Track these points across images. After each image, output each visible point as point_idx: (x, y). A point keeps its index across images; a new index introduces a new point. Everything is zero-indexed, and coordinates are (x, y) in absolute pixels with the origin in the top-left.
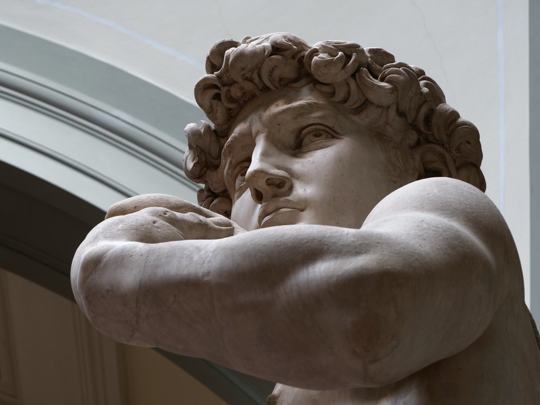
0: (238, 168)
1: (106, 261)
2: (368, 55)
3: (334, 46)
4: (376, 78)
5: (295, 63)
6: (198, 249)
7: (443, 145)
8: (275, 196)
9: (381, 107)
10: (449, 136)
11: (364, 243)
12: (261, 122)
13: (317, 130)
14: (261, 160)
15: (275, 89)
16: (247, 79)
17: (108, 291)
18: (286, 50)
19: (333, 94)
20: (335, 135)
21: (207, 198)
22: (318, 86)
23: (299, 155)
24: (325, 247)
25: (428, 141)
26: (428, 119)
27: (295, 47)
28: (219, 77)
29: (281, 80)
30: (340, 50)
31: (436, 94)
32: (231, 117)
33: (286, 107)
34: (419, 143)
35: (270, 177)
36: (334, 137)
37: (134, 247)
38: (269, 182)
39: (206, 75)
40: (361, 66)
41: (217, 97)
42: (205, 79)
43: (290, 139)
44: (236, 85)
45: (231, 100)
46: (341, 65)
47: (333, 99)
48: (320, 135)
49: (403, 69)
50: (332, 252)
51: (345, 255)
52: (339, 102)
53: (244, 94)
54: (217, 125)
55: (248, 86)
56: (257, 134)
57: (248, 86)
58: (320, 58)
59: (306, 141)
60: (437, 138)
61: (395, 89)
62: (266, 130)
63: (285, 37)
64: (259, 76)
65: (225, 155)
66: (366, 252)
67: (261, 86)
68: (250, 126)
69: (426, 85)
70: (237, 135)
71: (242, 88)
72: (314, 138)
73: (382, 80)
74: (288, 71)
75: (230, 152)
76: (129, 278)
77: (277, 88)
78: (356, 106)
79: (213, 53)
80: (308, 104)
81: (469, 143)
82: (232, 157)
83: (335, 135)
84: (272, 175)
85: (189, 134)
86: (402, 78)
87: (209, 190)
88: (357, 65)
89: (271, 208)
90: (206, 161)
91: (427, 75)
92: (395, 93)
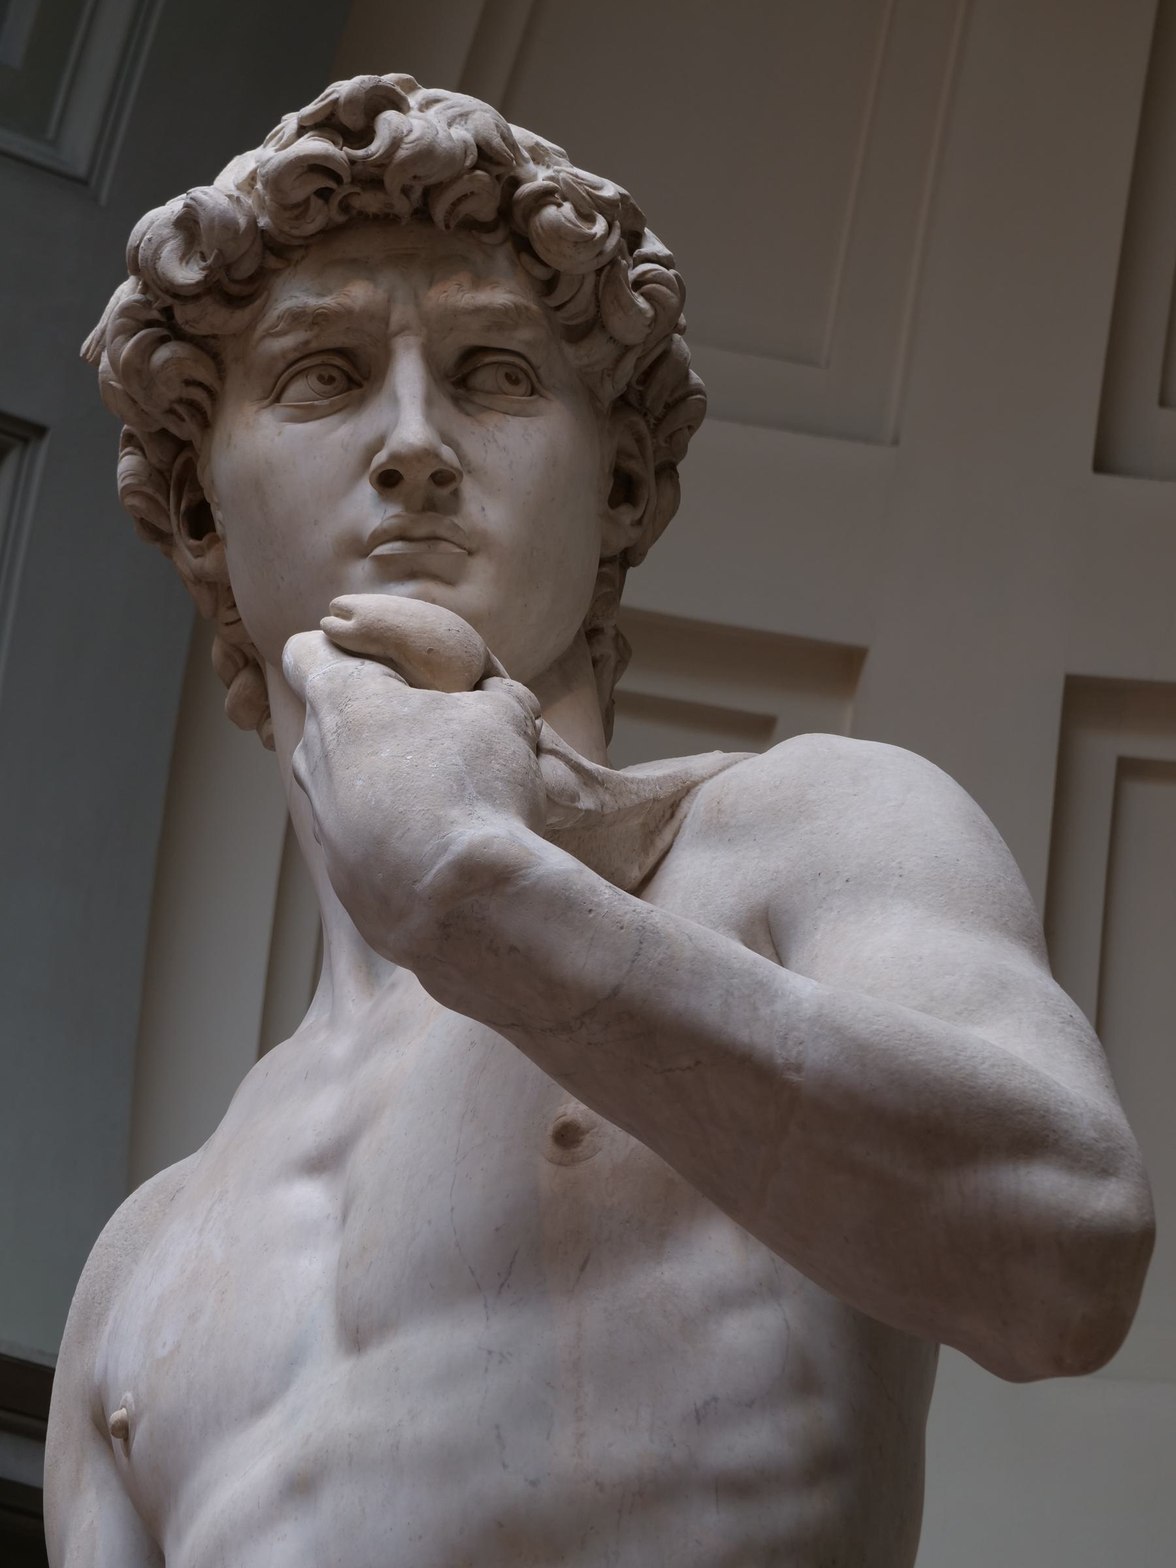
0: (317, 360)
3: (588, 193)
7: (645, 415)
8: (430, 506)
10: (670, 407)
15: (443, 228)
17: (513, 949)
18: (499, 164)
20: (537, 385)
21: (149, 324)
22: (525, 258)
28: (353, 162)
35: (443, 467)
36: (533, 392)
37: (593, 890)
41: (324, 194)
42: (327, 157)
48: (515, 382)
49: (676, 276)
56: (403, 329)
57: (402, 206)
58: (570, 221)
59: (485, 379)
60: (648, 404)
61: (655, 319)
68: (389, 301)
72: (507, 386)
74: (485, 209)
75: (314, 324)
76: (585, 962)
77: (447, 226)
78: (574, 322)
84: (445, 463)
85: (212, 220)
87: (168, 311)
89: (422, 530)
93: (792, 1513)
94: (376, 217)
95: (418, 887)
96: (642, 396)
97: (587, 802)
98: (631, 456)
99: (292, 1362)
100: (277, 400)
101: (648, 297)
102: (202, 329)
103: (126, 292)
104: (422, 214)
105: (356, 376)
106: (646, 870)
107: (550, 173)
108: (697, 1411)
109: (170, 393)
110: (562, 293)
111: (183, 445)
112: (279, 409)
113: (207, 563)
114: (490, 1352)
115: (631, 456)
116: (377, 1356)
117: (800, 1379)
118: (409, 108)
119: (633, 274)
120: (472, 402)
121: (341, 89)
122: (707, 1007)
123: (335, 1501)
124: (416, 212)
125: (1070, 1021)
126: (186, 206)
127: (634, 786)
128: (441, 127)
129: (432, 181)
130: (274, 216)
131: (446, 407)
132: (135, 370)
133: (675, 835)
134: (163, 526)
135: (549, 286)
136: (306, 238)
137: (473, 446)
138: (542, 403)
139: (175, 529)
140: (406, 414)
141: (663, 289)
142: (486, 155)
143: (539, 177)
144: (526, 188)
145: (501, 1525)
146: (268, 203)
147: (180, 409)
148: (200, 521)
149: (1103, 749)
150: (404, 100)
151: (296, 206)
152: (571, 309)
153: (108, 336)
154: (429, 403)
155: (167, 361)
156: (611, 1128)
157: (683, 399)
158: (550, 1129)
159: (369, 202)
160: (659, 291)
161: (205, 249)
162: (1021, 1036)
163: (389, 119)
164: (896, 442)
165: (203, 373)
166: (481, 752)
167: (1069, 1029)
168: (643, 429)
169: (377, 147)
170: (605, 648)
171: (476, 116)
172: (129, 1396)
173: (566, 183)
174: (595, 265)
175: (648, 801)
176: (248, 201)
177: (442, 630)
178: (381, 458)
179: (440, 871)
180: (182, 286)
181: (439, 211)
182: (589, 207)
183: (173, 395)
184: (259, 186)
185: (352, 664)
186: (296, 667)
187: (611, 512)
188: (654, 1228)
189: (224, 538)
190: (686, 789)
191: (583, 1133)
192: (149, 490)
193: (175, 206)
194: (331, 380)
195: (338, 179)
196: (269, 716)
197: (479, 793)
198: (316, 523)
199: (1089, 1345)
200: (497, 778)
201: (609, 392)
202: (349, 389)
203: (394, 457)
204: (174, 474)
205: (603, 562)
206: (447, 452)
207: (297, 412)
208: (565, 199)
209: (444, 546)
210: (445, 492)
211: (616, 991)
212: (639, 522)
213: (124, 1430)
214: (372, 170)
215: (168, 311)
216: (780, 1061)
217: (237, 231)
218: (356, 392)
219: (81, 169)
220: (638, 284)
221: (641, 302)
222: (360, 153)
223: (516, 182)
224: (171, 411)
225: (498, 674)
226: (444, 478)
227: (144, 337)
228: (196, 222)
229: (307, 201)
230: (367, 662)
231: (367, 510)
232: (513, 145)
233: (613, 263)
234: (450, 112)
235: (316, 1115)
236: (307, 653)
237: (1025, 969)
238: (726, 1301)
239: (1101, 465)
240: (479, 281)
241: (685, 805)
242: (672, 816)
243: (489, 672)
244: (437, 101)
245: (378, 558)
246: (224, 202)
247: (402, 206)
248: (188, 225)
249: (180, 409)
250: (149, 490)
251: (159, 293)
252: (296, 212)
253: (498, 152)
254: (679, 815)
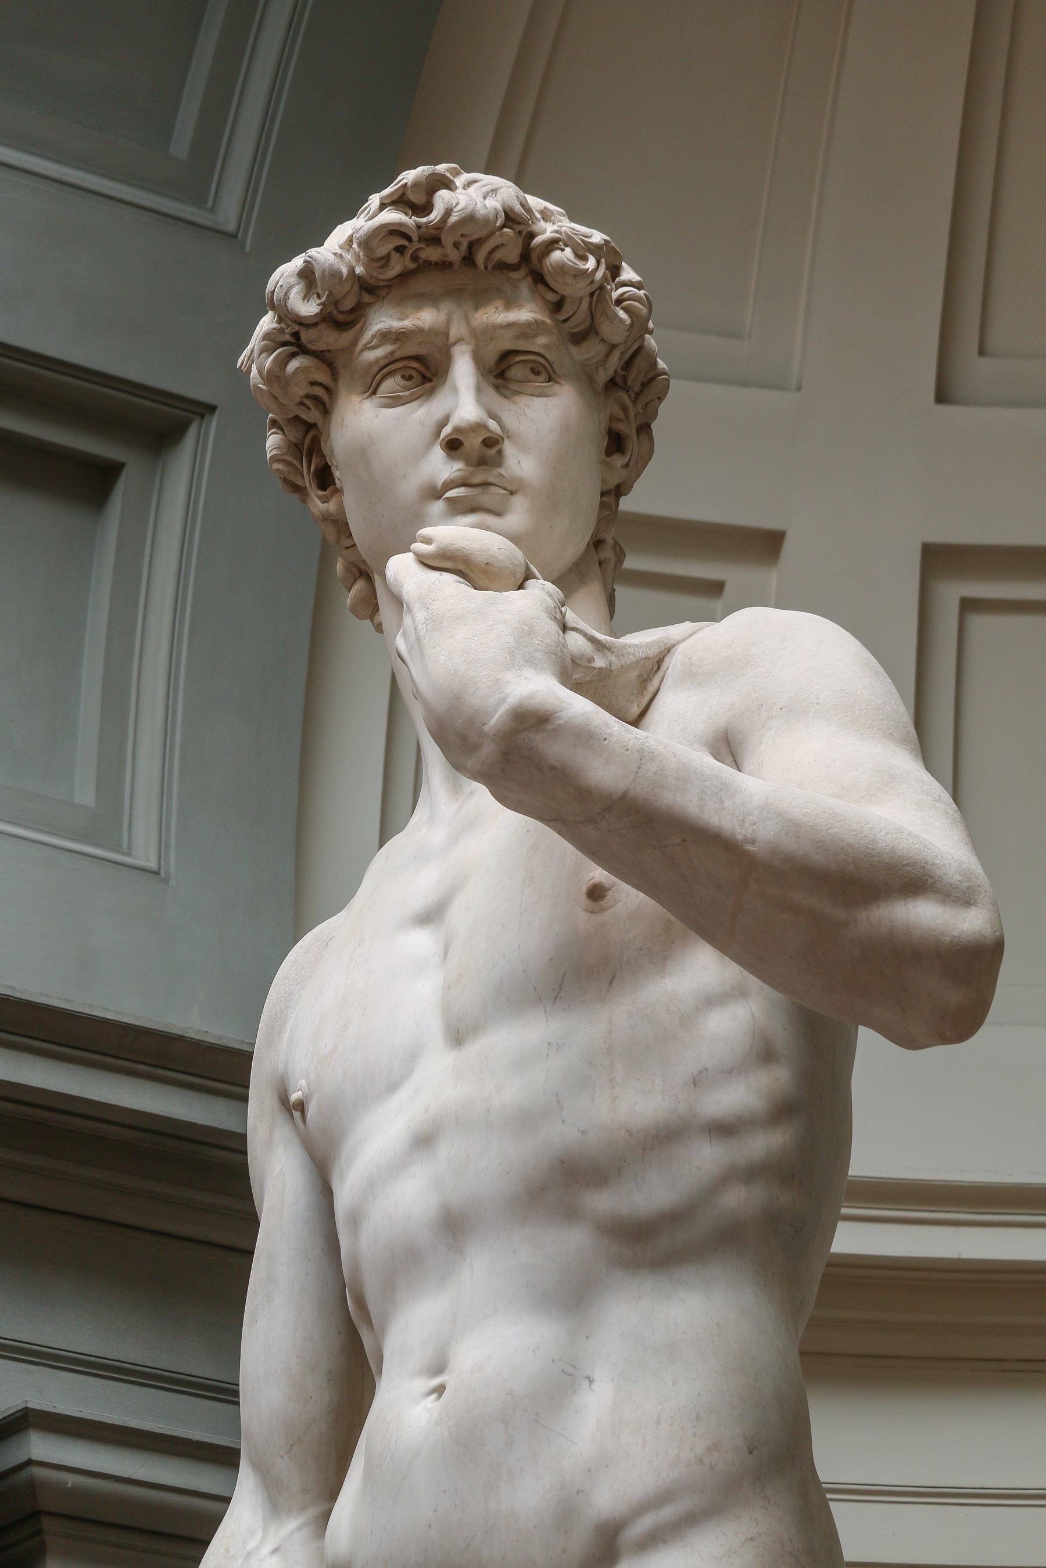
1: (560, 725)
3: (582, 240)
8: (482, 462)
10: (646, 385)
12: (468, 323)
17: (553, 768)
18: (519, 223)
20: (553, 375)
21: (284, 344)
22: (541, 287)
23: (507, 392)
24: (930, 881)
28: (419, 226)
36: (550, 379)
37: (607, 725)
41: (400, 250)
42: (401, 224)
44: (439, 250)
48: (537, 373)
50: (937, 891)
56: (459, 341)
57: (454, 256)
59: (516, 372)
60: (629, 383)
61: (632, 325)
70: (426, 328)
72: (532, 376)
74: (512, 255)
76: (604, 774)
77: (486, 268)
78: (576, 330)
79: (416, 184)
82: (399, 348)
85: (324, 270)
87: (296, 335)
89: (478, 479)
93: (763, 1144)
94: (436, 263)
95: (486, 728)
96: (625, 378)
97: (600, 663)
98: (619, 420)
99: (412, 1057)
100: (374, 393)
101: (626, 310)
102: (320, 346)
103: (267, 322)
104: (469, 260)
105: (428, 374)
106: (642, 707)
107: (555, 227)
108: (694, 1078)
109: (300, 390)
110: (567, 311)
111: (310, 426)
112: (376, 399)
113: (331, 506)
114: (549, 1044)
115: (619, 420)
116: (473, 1049)
117: (765, 1054)
118: (456, 188)
119: (615, 295)
120: (509, 389)
121: (409, 176)
122: (690, 803)
123: (448, 1150)
124: (464, 259)
125: (939, 799)
126: (306, 262)
127: (631, 650)
128: (479, 199)
129: (475, 237)
130: (366, 266)
131: (490, 392)
132: (274, 377)
133: (661, 682)
134: (300, 483)
135: (557, 306)
136: (389, 280)
137: (510, 419)
138: (556, 387)
139: (308, 484)
140: (463, 399)
141: (637, 304)
142: (510, 218)
143: (547, 231)
144: (538, 239)
145: (562, 1162)
146: (362, 257)
147: (308, 402)
148: (325, 478)
149: (950, 593)
150: (453, 182)
151: (381, 259)
152: (574, 320)
153: (256, 354)
154: (479, 390)
155: (297, 369)
156: (625, 887)
157: (653, 379)
158: (585, 888)
159: (432, 254)
160: (634, 306)
161: (320, 291)
162: (906, 812)
163: (442, 197)
164: (799, 388)
165: (323, 377)
166: (526, 632)
167: (939, 805)
168: (626, 403)
169: (435, 215)
170: (607, 553)
171: (502, 191)
172: (303, 1082)
173: (567, 234)
174: (589, 290)
175: (642, 659)
176: (348, 256)
177: (494, 549)
178: (447, 430)
179: (500, 716)
180: (305, 317)
181: (480, 257)
182: (583, 250)
183: (302, 393)
184: (355, 246)
185: (436, 574)
186: (396, 579)
187: (608, 459)
188: (659, 952)
189: (342, 488)
190: (668, 650)
191: (608, 890)
192: (289, 458)
193: (298, 262)
194: (410, 378)
195: (409, 238)
196: (378, 610)
197: (525, 661)
198: (404, 476)
199: (961, 1022)
200: (537, 650)
201: (603, 377)
202: (423, 384)
203: (457, 430)
204: (305, 446)
205: (603, 494)
206: (492, 424)
207: (389, 401)
208: (566, 245)
209: (493, 489)
210: (492, 452)
211: (625, 794)
212: (627, 465)
213: (301, 1106)
214: (432, 231)
215: (296, 335)
216: (740, 837)
217: (341, 278)
218: (428, 385)
219: (231, 227)
220: (619, 302)
221: (622, 314)
222: (424, 220)
223: (532, 235)
224: (301, 403)
225: (535, 577)
226: (491, 442)
227: (280, 353)
228: (313, 273)
229: (389, 255)
230: (444, 574)
231: (441, 467)
232: (529, 210)
233: (601, 288)
234: (485, 189)
235: (423, 885)
236: (402, 569)
237: (906, 764)
238: (711, 1001)
239: (942, 397)
240: (510, 304)
241: (667, 660)
242: (659, 668)
243: (528, 576)
244: (475, 182)
245: (447, 499)
246: (332, 258)
247: (454, 256)
248: (307, 274)
249: (308, 402)
250: (289, 458)
251: (290, 323)
252: (381, 263)
253: (519, 215)
254: (663, 668)
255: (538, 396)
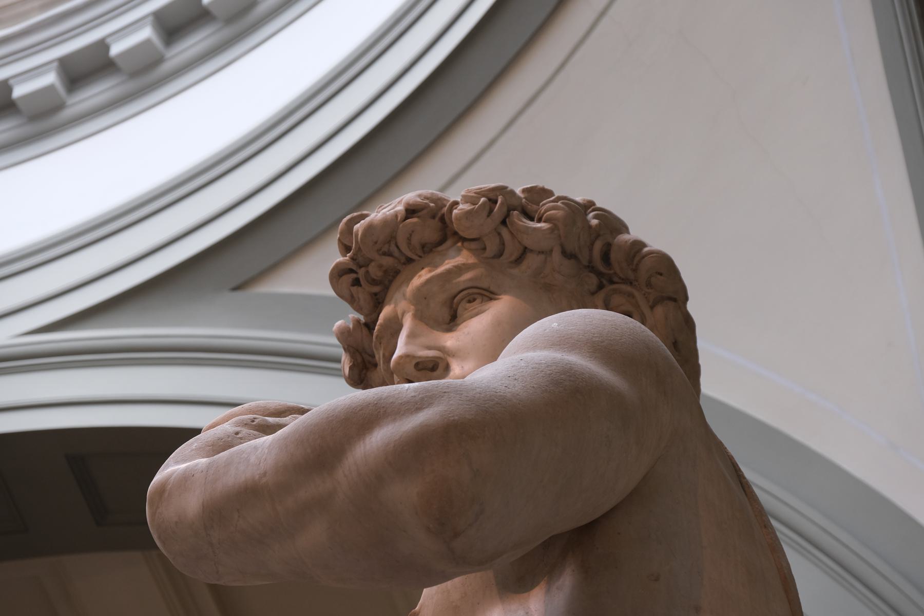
2: (522, 195)
4: (532, 219)
5: (435, 223)
6: (256, 448)
7: (631, 283)
9: (543, 252)
10: (635, 270)
11: (426, 396)
13: (469, 294)
14: (407, 344)
16: (384, 254)
18: (422, 209)
19: (484, 249)
22: (466, 244)
25: (612, 282)
26: (606, 257)
27: (432, 205)
28: (352, 259)
29: (423, 246)
30: (484, 196)
31: (612, 225)
32: (379, 303)
33: (429, 275)
34: (601, 287)
35: (418, 360)
36: (491, 299)
37: (197, 465)
38: (420, 366)
39: (340, 259)
40: (510, 209)
41: (356, 282)
43: (445, 314)
44: (373, 264)
45: (374, 282)
46: (485, 213)
47: (485, 255)
48: (474, 300)
51: (403, 415)
52: (494, 257)
53: (386, 272)
54: (366, 316)
55: (387, 261)
57: (387, 261)
60: (621, 275)
62: (412, 307)
63: (420, 196)
64: (397, 247)
65: (377, 349)
66: (430, 405)
67: (403, 260)
69: (595, 217)
71: (380, 266)
72: (468, 305)
73: (539, 221)
74: (429, 232)
78: (514, 258)
80: (456, 267)
81: (661, 274)
83: (492, 296)
84: (420, 357)
86: (559, 213)
88: (505, 209)
90: (363, 361)
91: (598, 205)
92: (556, 232)
157: (640, 261)
163: (359, 227)
255: (477, 314)
